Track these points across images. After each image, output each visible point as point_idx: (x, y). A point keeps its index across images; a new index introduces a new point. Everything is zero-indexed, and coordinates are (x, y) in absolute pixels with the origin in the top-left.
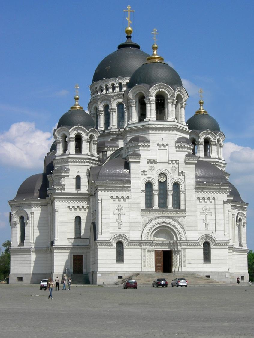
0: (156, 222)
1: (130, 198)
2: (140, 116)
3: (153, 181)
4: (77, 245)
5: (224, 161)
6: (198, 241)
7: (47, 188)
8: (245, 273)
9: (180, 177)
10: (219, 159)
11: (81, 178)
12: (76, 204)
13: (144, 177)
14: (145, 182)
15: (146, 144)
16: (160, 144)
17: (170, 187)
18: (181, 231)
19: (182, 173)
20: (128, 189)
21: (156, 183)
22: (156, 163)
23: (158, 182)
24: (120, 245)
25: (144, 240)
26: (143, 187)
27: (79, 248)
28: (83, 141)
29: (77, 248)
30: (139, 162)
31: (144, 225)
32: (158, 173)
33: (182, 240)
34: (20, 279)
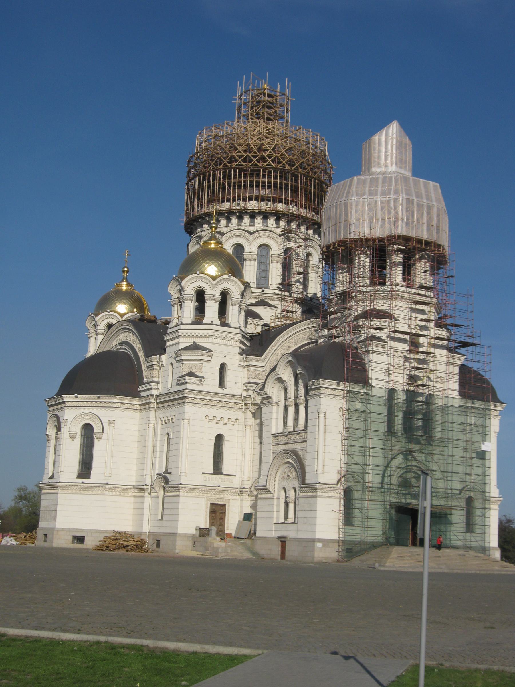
12: (219, 413)
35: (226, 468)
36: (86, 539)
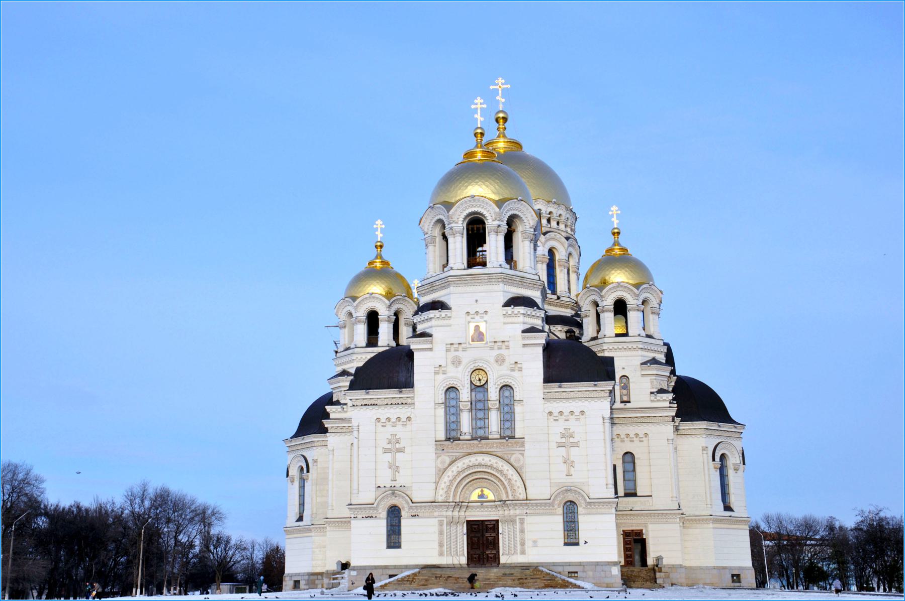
1: (412, 420)
5: (663, 340)
8: (745, 568)
9: (513, 373)
10: (648, 336)
13: (441, 377)
14: (444, 387)
15: (443, 315)
16: (472, 312)
21: (466, 387)
22: (464, 350)
24: (394, 513)
25: (440, 501)
26: (441, 398)
30: (431, 349)
32: (469, 368)
33: (516, 498)
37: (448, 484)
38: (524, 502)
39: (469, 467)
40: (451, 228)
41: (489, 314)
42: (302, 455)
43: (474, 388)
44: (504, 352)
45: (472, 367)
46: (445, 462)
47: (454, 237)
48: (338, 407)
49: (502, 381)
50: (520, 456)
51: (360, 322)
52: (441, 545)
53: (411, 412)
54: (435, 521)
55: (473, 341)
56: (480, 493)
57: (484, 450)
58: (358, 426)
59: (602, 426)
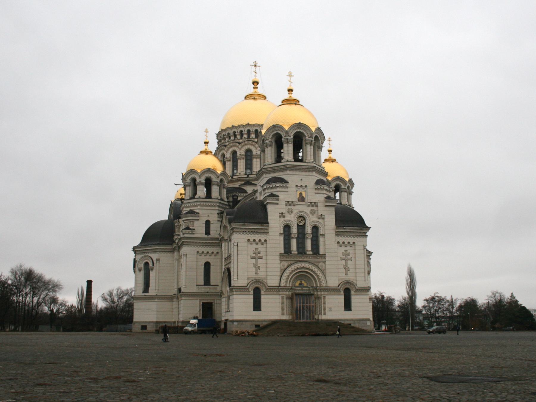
0: (295, 266)
1: (268, 241)
2: (276, 157)
3: (291, 224)
4: (206, 292)
6: (339, 286)
7: (174, 234)
11: (211, 223)
12: (205, 249)
13: (282, 219)
16: (299, 185)
17: (309, 230)
18: (321, 277)
19: (322, 217)
20: (266, 232)
22: (294, 205)
23: (296, 225)
27: (208, 295)
28: (213, 185)
29: (206, 295)
30: (277, 204)
31: (283, 271)
33: (322, 286)
34: (144, 327)
35: (212, 282)
36: (148, 327)
37: (287, 277)
38: (326, 288)
39: (298, 269)
40: (287, 139)
41: (308, 187)
42: (149, 256)
43: (298, 225)
44: (315, 208)
45: (298, 215)
46: (285, 265)
47: (288, 144)
48: (190, 231)
49: (314, 224)
50: (323, 264)
51: (201, 183)
52: (283, 310)
53: (267, 237)
54: (278, 297)
55: (299, 201)
56: (300, 283)
57: (305, 260)
58: (238, 243)
59: (363, 250)
